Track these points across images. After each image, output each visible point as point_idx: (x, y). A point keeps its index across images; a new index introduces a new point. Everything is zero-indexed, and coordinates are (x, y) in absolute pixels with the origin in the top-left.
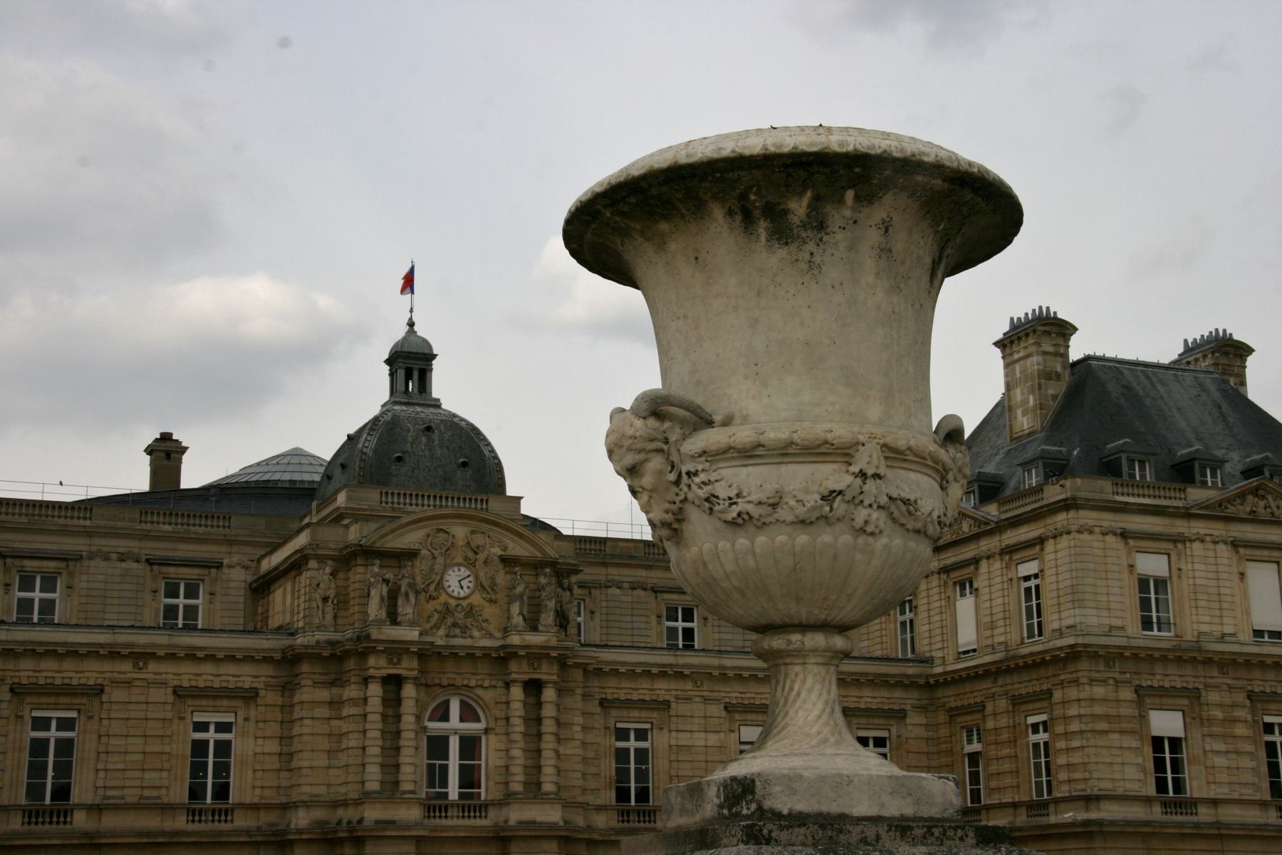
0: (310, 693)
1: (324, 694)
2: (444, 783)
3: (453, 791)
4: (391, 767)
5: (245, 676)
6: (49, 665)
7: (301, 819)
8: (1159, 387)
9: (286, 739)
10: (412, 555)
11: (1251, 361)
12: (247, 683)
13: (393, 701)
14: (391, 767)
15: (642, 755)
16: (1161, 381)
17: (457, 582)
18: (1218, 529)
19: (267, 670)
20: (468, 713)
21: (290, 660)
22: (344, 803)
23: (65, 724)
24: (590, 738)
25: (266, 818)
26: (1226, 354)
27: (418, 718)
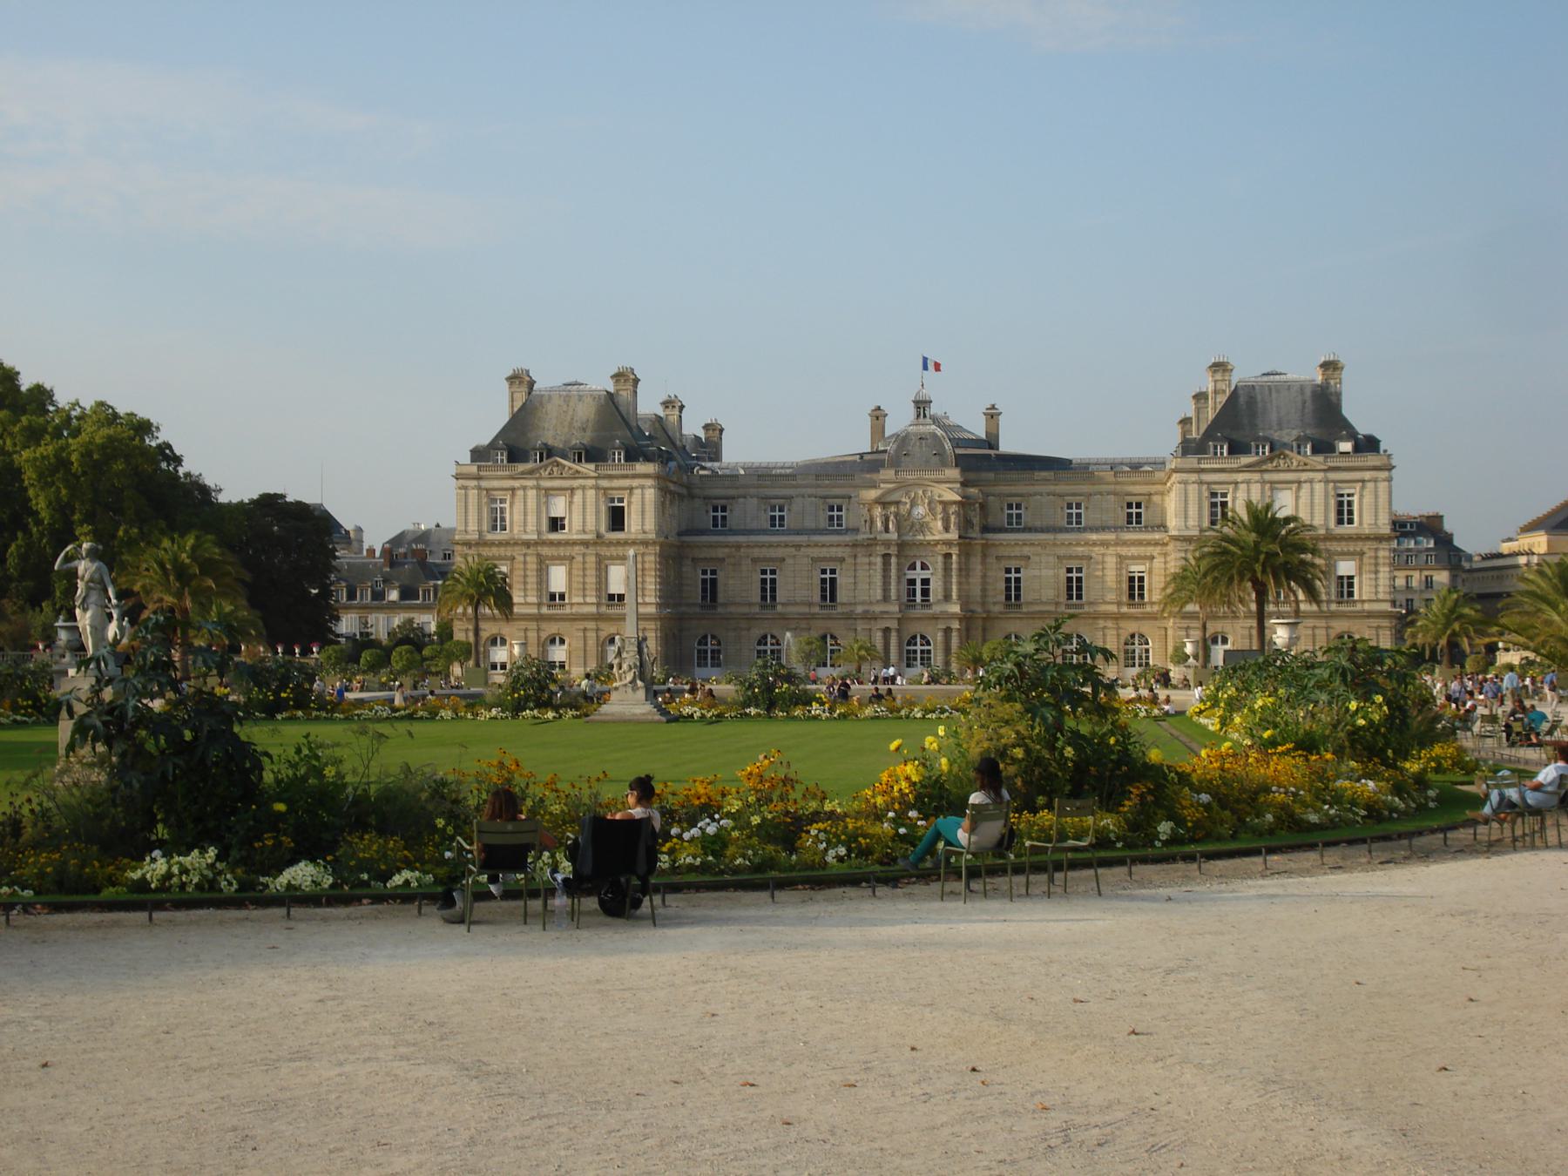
0: (862, 560)
1: (866, 560)
3: (919, 598)
4: (886, 590)
6: (764, 550)
7: (859, 609)
8: (1274, 395)
10: (897, 503)
14: (886, 590)
15: (1018, 580)
16: (1278, 391)
18: (1256, 476)
19: (848, 550)
21: (855, 546)
22: (871, 603)
23: (773, 572)
26: (1330, 366)
27: (899, 570)
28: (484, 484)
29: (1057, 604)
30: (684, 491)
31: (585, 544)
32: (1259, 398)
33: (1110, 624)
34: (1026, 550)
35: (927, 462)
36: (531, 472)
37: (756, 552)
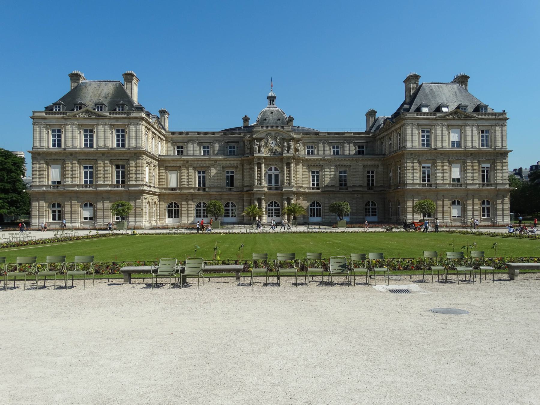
1: (248, 167)
2: (272, 183)
3: (273, 184)
5: (235, 163)
6: (200, 162)
7: (245, 189)
9: (243, 175)
11: (469, 80)
12: (236, 165)
13: (259, 167)
15: (317, 177)
17: (272, 143)
19: (239, 162)
20: (276, 169)
24: (304, 173)
25: (240, 190)
28: (47, 121)
29: (336, 187)
30: (164, 138)
31: (103, 154)
32: (435, 90)
33: (359, 196)
34: (321, 163)
35: (276, 123)
36: (74, 116)
37: (196, 163)
